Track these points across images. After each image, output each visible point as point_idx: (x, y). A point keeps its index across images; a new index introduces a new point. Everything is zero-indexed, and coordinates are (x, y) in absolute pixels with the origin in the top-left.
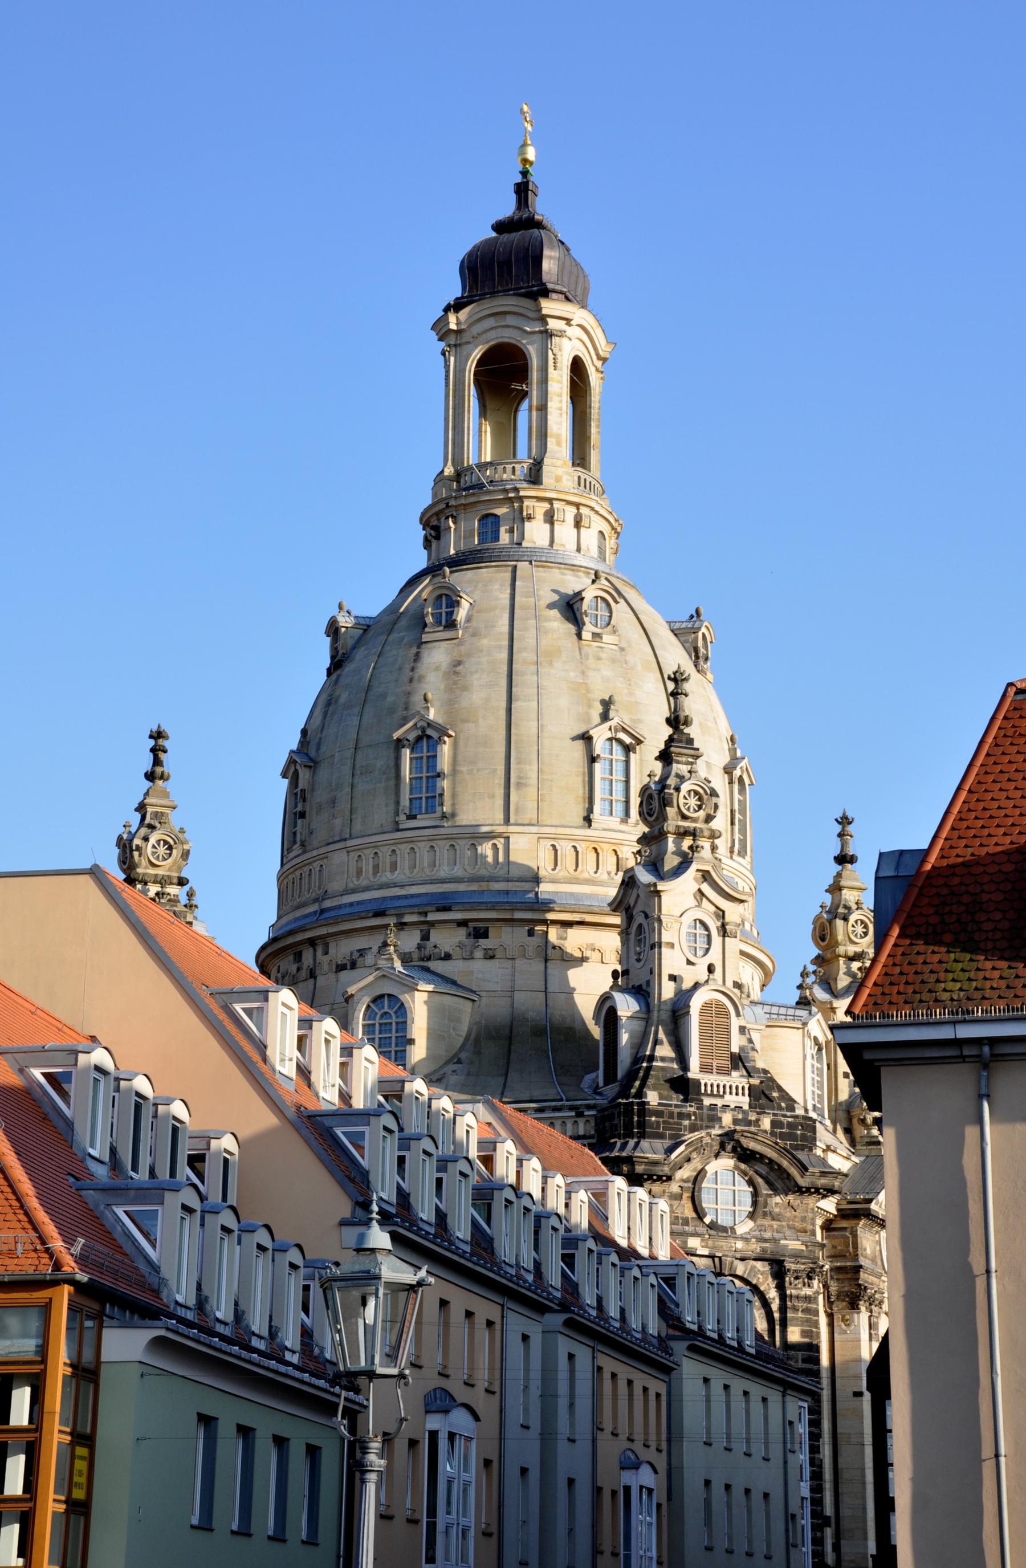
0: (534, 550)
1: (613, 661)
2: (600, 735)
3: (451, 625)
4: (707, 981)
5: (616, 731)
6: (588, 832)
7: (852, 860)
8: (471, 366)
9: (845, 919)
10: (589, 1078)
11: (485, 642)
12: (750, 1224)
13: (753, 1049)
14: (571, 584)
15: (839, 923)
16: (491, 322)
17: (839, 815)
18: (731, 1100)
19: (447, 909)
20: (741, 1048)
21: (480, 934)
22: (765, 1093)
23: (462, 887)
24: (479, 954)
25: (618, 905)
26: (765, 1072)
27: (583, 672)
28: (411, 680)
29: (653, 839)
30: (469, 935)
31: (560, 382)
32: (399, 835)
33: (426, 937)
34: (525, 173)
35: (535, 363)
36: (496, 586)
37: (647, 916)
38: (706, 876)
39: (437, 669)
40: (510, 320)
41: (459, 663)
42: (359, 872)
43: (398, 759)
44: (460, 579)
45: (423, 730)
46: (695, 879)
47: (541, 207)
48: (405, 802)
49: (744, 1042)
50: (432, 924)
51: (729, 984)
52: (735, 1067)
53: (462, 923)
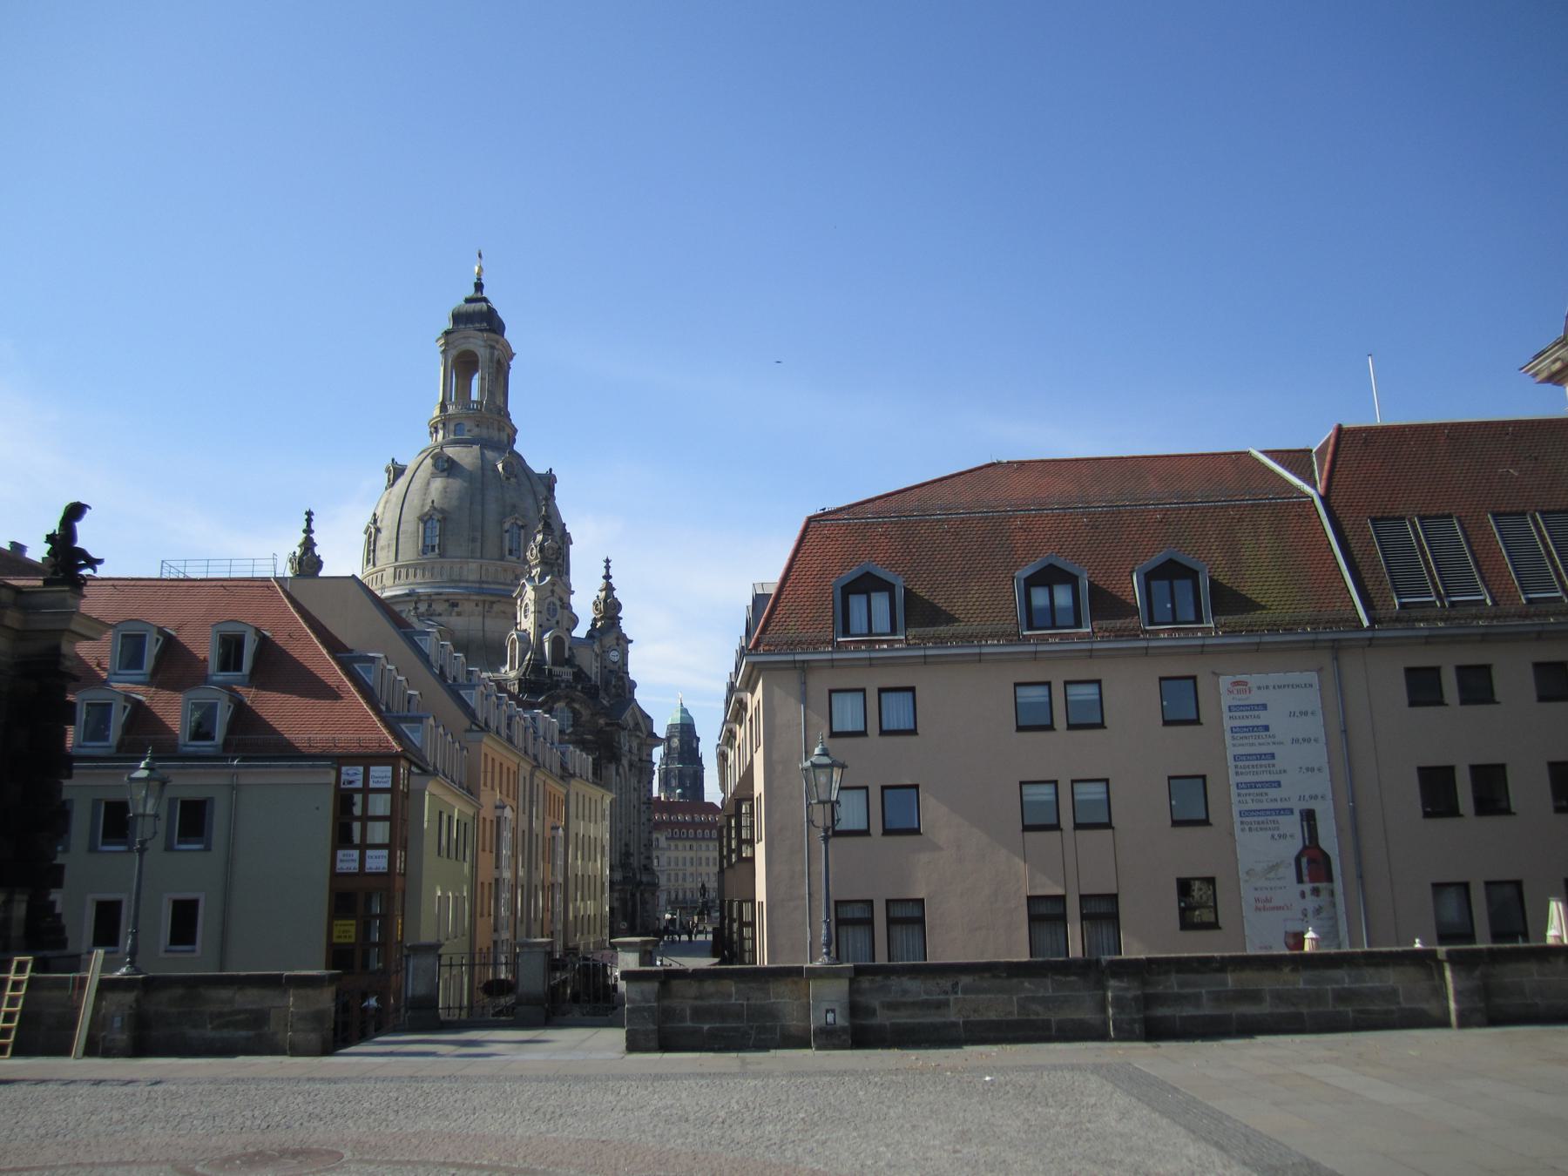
21: (455, 605)
22: (580, 675)
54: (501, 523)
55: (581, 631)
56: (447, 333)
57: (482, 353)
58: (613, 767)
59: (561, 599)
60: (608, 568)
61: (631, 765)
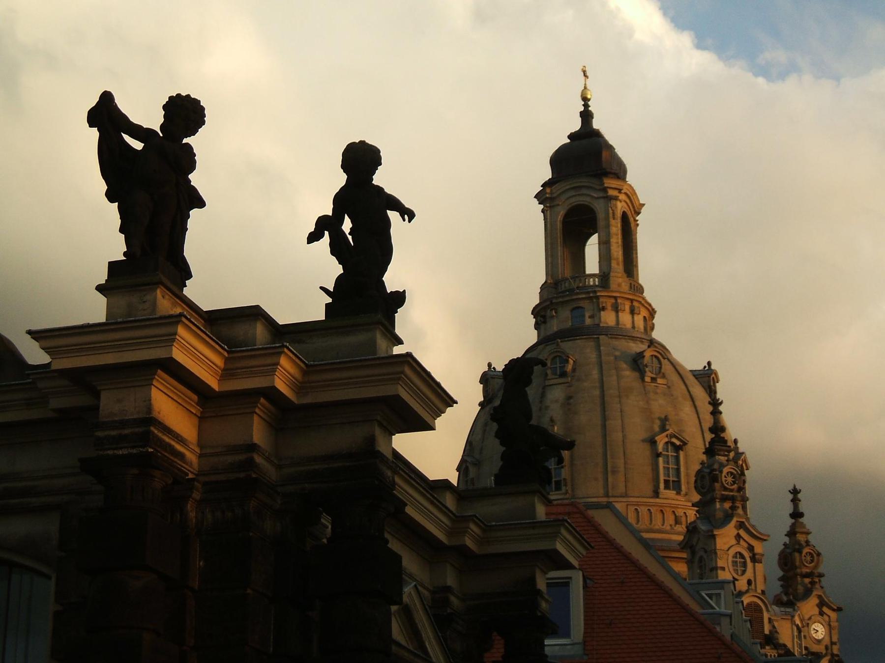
0: (608, 328)
1: (664, 395)
2: (661, 440)
3: (563, 374)
4: (747, 591)
5: (671, 437)
6: (657, 500)
7: (801, 515)
8: (560, 218)
9: (800, 552)
11: (585, 384)
13: (776, 632)
14: (636, 347)
15: (797, 555)
16: (573, 193)
17: (791, 488)
20: (770, 631)
25: (687, 545)
27: (648, 402)
28: (540, 409)
29: (704, 506)
31: (617, 227)
34: (586, 106)
35: (601, 215)
36: (588, 350)
37: (706, 552)
38: (741, 525)
39: (557, 401)
40: (584, 191)
41: (570, 398)
44: (567, 346)
46: (735, 527)
47: (596, 124)
51: (759, 591)
57: (599, 207)
60: (795, 501)
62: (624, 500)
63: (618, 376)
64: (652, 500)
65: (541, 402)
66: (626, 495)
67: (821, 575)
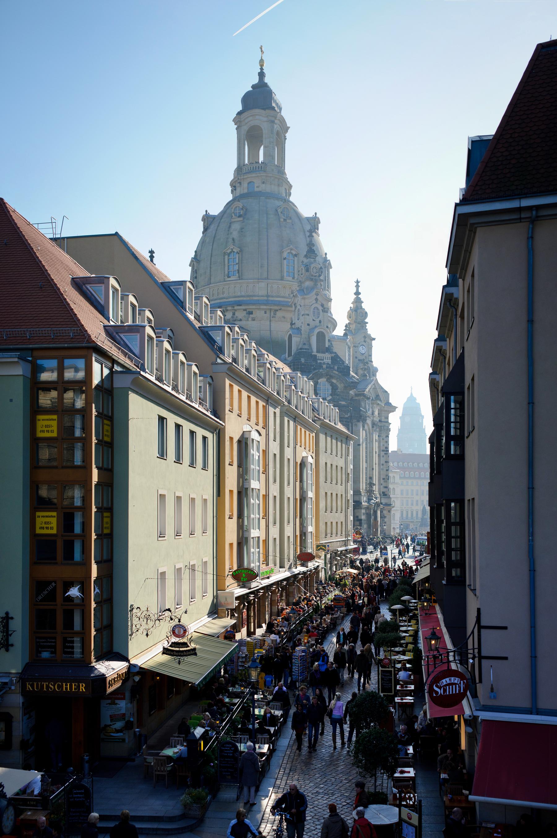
6: (283, 282)
7: (360, 294)
10: (283, 356)
12: (331, 397)
18: (326, 361)
19: (240, 305)
21: (251, 313)
22: (336, 359)
23: (245, 299)
24: (250, 319)
26: (336, 353)
30: (247, 313)
32: (225, 283)
33: (234, 314)
40: (257, 117)
42: (213, 295)
43: (224, 259)
45: (232, 249)
48: (226, 272)
49: (330, 344)
50: (236, 310)
52: (327, 352)
53: (245, 310)
54: (281, 252)
55: (339, 331)
56: (239, 113)
57: (265, 127)
58: (361, 424)
59: (322, 305)
60: (357, 286)
61: (374, 424)
62: (266, 281)
63: (267, 217)
64: (280, 281)
65: (228, 231)
66: (268, 279)
67: (367, 323)
